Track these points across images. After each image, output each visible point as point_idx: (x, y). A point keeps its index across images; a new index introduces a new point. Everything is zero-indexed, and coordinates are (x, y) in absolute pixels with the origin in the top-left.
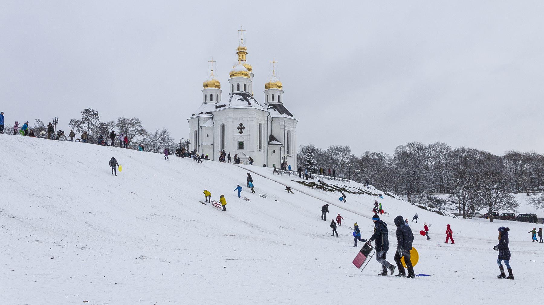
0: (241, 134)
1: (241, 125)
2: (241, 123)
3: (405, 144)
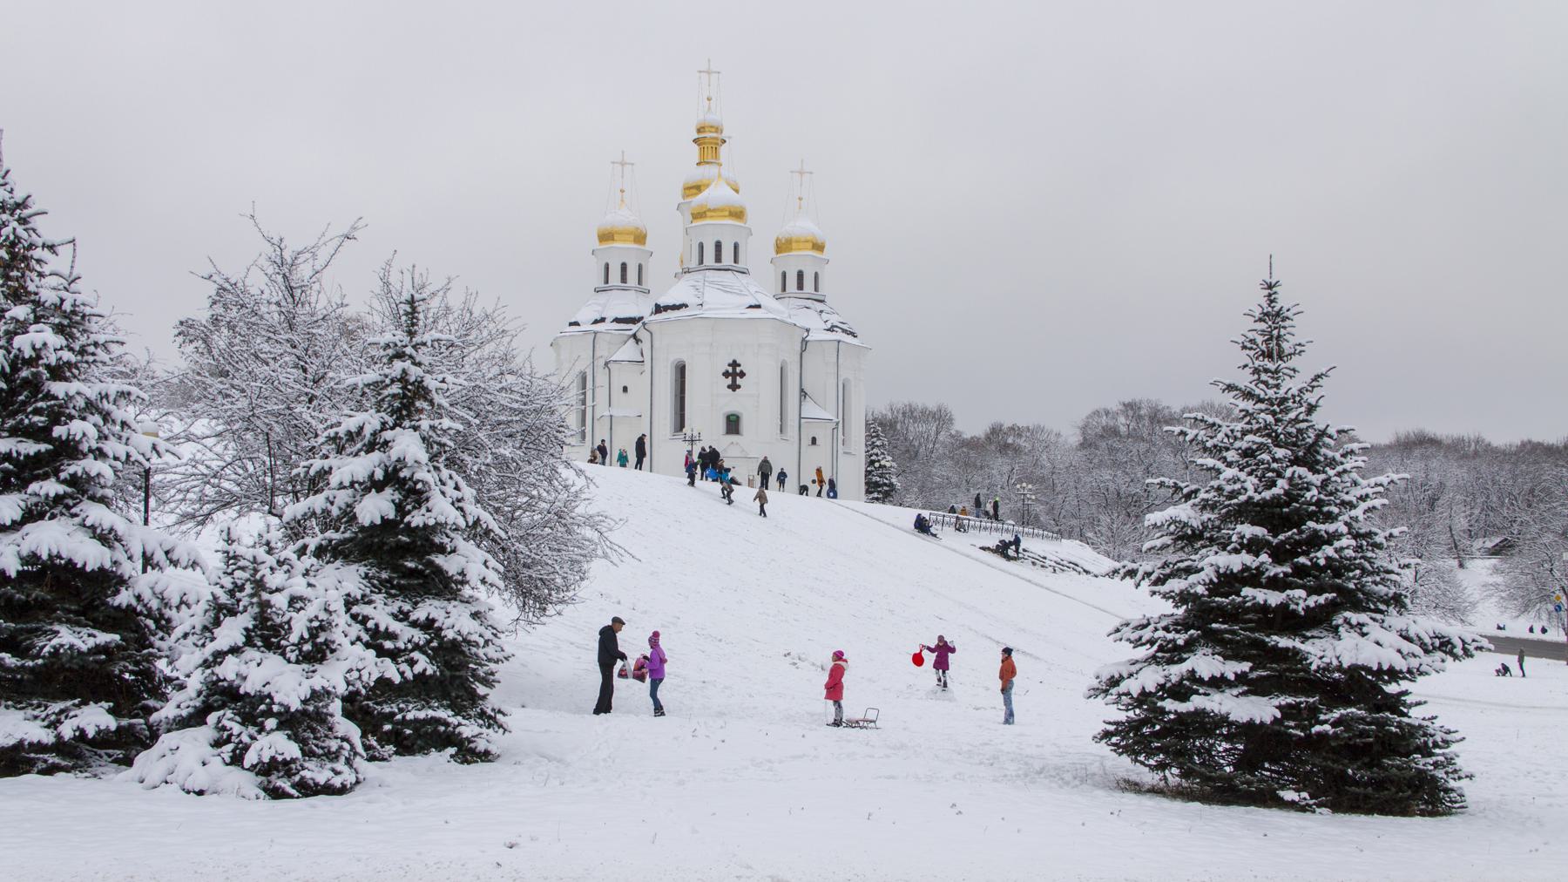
0: (734, 390)
1: (735, 364)
2: (734, 362)
3: (1114, 406)
